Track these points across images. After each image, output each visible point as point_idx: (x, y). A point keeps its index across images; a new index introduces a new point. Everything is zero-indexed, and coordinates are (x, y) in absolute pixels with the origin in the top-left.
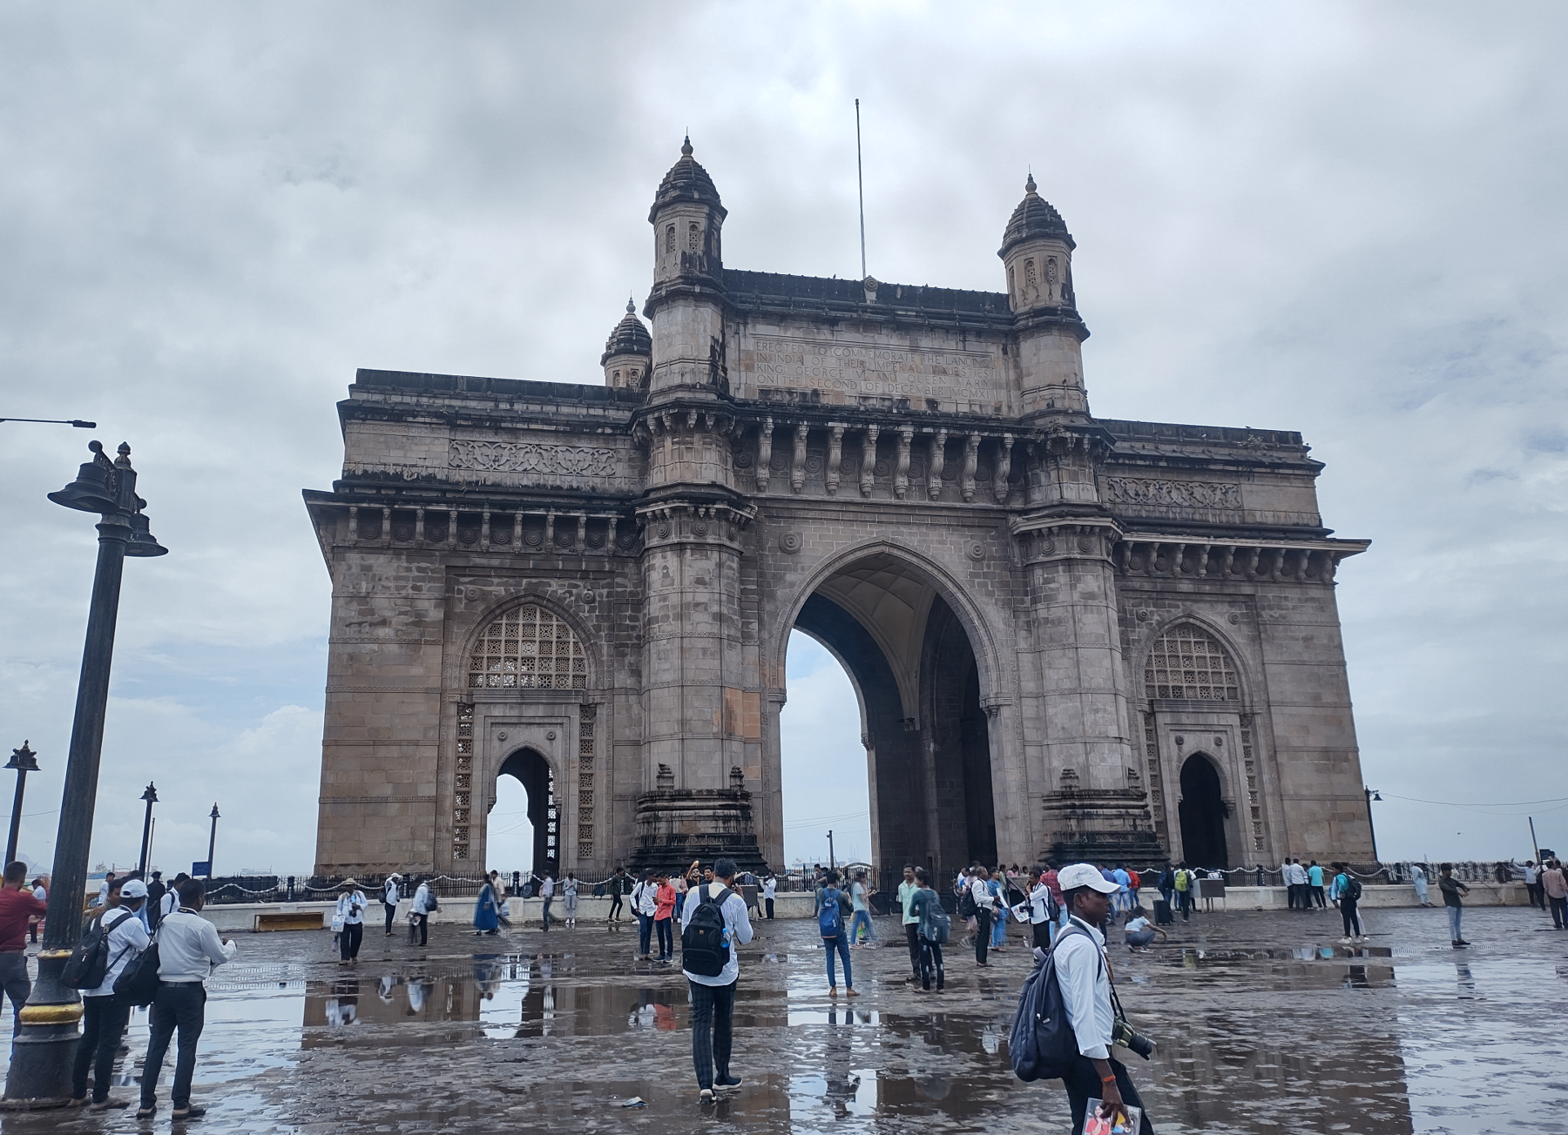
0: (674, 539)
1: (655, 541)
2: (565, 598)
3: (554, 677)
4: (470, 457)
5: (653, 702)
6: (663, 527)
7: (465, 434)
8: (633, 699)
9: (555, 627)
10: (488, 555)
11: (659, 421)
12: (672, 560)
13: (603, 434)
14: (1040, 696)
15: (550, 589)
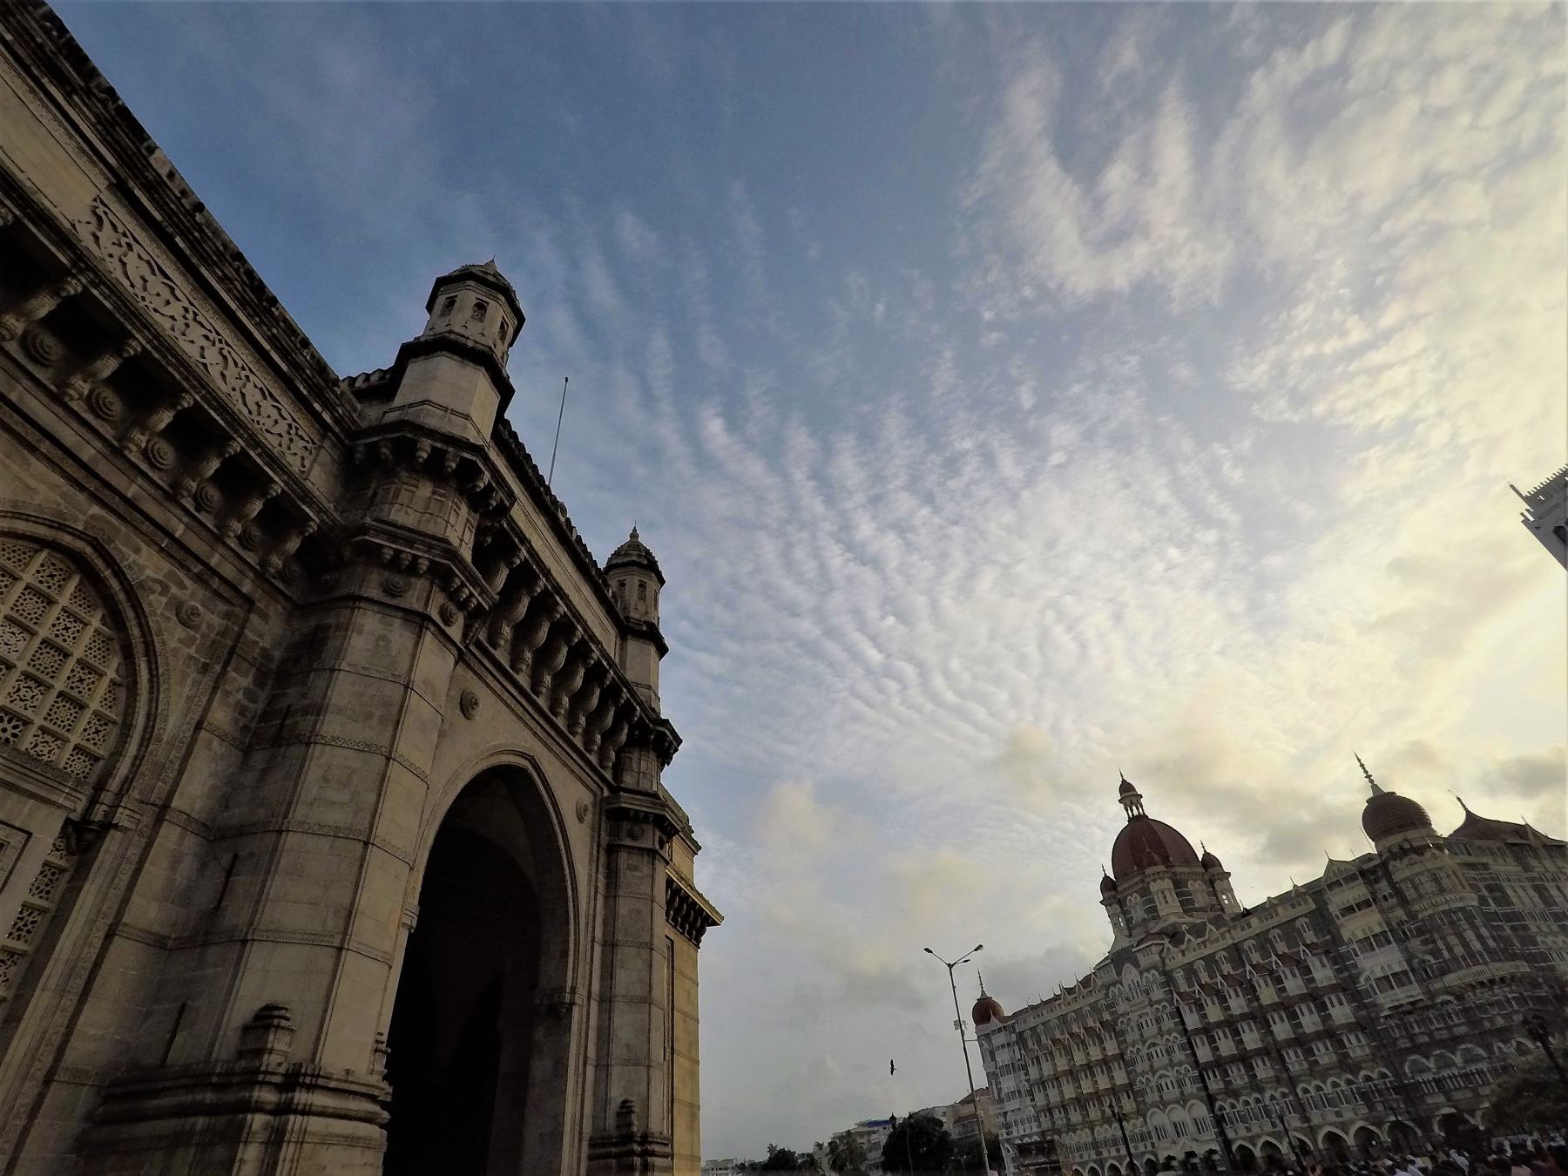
0: (413, 600)
1: (374, 592)
2: (153, 592)
3: (33, 730)
4: (117, 251)
5: (285, 861)
6: (398, 579)
7: (130, 220)
8: (191, 843)
9: (90, 632)
10: (61, 412)
11: (437, 457)
12: (400, 636)
13: (317, 417)
14: (607, 1001)
15: (132, 557)
